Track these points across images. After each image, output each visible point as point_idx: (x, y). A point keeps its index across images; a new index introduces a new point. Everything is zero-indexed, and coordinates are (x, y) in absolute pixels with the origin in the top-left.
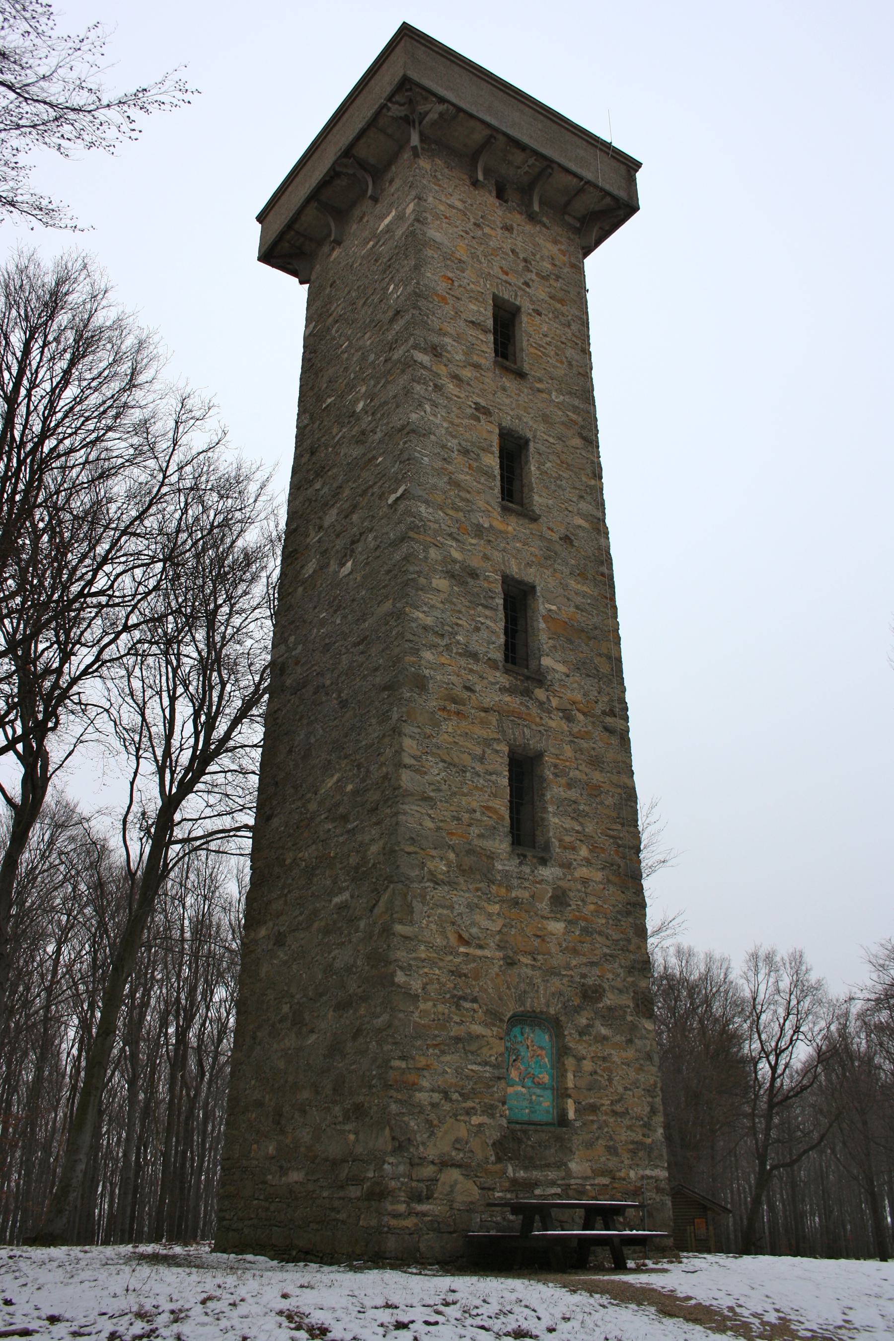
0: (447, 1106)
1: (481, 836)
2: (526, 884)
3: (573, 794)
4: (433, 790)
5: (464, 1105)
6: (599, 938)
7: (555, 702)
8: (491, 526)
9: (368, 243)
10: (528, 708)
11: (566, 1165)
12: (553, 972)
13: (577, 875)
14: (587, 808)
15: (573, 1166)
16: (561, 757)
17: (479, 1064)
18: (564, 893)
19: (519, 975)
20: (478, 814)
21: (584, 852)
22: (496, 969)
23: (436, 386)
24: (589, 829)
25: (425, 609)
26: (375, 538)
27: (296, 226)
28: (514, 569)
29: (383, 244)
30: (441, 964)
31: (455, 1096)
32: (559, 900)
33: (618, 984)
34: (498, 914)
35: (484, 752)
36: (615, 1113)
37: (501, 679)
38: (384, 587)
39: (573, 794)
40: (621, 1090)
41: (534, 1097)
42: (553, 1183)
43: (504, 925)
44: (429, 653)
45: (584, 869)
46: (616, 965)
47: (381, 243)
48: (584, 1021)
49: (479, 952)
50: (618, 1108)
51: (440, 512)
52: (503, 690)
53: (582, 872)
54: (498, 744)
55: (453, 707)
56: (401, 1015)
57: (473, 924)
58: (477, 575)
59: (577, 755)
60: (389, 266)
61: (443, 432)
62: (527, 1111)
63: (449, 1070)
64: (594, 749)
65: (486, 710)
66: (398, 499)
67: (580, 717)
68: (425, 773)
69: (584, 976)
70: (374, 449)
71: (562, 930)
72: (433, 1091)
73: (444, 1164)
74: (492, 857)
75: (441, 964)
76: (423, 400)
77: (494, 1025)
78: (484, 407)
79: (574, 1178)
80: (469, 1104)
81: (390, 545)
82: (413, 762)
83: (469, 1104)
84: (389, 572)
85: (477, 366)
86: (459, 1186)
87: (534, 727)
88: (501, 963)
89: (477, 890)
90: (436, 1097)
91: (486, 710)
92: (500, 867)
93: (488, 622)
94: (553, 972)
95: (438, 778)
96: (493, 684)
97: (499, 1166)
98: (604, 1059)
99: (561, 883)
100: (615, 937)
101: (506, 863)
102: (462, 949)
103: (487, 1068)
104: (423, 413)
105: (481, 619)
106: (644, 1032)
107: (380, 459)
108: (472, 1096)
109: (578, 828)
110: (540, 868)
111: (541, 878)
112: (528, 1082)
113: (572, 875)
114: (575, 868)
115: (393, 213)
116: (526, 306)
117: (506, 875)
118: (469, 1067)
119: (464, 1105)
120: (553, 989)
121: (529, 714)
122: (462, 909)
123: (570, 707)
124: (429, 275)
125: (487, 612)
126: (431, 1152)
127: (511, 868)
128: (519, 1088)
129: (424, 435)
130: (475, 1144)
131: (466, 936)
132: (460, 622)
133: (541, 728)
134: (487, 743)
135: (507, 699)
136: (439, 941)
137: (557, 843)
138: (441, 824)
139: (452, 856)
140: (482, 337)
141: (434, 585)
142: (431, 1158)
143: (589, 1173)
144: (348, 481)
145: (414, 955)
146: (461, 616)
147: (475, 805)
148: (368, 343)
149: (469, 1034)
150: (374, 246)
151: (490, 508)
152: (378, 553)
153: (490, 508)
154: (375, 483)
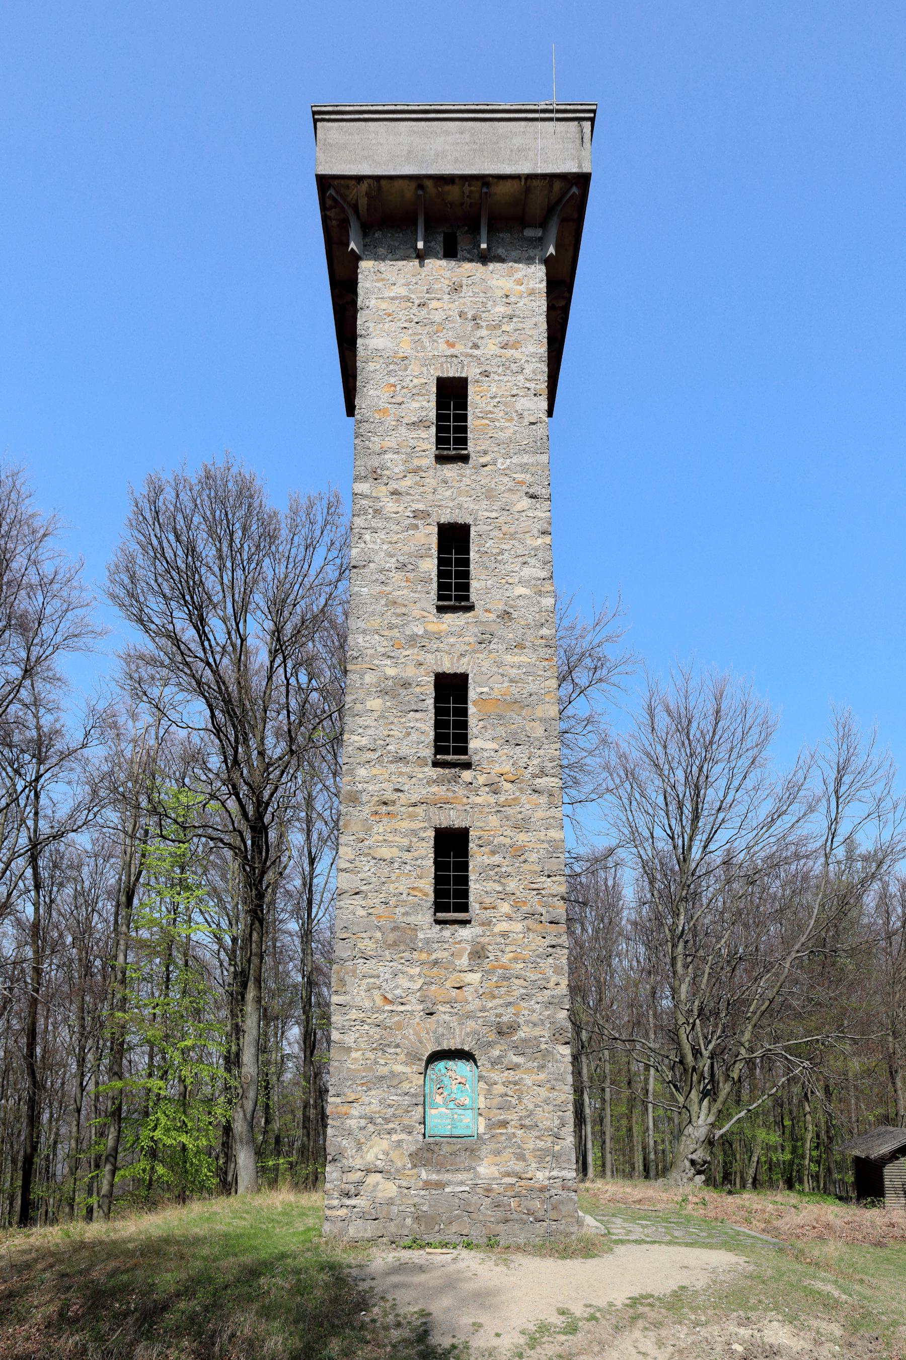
0: (371, 1128)
1: (406, 914)
2: (446, 946)
3: (496, 859)
5: (386, 1127)
6: (517, 981)
7: (482, 779)
8: (426, 631)
10: (454, 792)
11: (474, 1168)
12: (469, 1016)
13: (497, 929)
14: (509, 869)
15: (481, 1170)
16: (487, 828)
17: (400, 1095)
18: (483, 948)
19: (438, 1021)
20: (404, 895)
21: (505, 908)
22: (417, 1020)
23: (376, 511)
24: (512, 885)
25: (360, 731)
28: (448, 667)
30: (369, 1021)
31: (379, 1120)
32: (478, 954)
33: (535, 1017)
34: (419, 975)
35: (411, 841)
36: (522, 1126)
37: (430, 773)
39: (496, 859)
40: (531, 1106)
42: (462, 1183)
43: (425, 983)
44: (363, 769)
45: (504, 923)
46: (532, 1002)
48: (496, 1053)
49: (402, 1008)
50: (527, 1122)
51: (376, 637)
52: (431, 782)
53: (503, 926)
54: (425, 832)
55: (384, 809)
56: (336, 1064)
57: (396, 987)
58: (409, 684)
61: (382, 554)
68: (359, 872)
69: (499, 1015)
71: (479, 980)
72: (360, 1118)
73: (368, 1171)
74: (415, 928)
75: (369, 1021)
76: (363, 531)
77: (414, 1064)
78: (423, 512)
79: (482, 1179)
80: (391, 1125)
82: (348, 865)
83: (391, 1125)
86: (380, 1187)
87: (459, 807)
88: (422, 1013)
89: (402, 958)
90: (363, 1122)
93: (418, 725)
94: (469, 1016)
95: (369, 874)
97: (415, 1171)
98: (516, 1083)
99: (482, 940)
100: (533, 978)
101: (428, 931)
102: (388, 1008)
103: (406, 1097)
104: (363, 545)
105: (412, 725)
108: (393, 1119)
109: (500, 889)
110: (460, 930)
114: (495, 925)
117: (427, 941)
119: (386, 1127)
120: (468, 1030)
121: (457, 798)
122: (387, 976)
123: (498, 779)
125: (418, 715)
126: (358, 1163)
127: (433, 936)
129: (364, 566)
130: (394, 1155)
131: (389, 996)
132: (391, 733)
133: (467, 807)
134: (414, 832)
135: (434, 789)
136: (367, 1004)
137: (477, 906)
138: (370, 911)
139: (378, 935)
141: (368, 708)
142: (358, 1167)
145: (348, 1017)
146: (393, 727)
147: (401, 889)
149: (391, 1072)
151: (426, 614)
153: (426, 614)
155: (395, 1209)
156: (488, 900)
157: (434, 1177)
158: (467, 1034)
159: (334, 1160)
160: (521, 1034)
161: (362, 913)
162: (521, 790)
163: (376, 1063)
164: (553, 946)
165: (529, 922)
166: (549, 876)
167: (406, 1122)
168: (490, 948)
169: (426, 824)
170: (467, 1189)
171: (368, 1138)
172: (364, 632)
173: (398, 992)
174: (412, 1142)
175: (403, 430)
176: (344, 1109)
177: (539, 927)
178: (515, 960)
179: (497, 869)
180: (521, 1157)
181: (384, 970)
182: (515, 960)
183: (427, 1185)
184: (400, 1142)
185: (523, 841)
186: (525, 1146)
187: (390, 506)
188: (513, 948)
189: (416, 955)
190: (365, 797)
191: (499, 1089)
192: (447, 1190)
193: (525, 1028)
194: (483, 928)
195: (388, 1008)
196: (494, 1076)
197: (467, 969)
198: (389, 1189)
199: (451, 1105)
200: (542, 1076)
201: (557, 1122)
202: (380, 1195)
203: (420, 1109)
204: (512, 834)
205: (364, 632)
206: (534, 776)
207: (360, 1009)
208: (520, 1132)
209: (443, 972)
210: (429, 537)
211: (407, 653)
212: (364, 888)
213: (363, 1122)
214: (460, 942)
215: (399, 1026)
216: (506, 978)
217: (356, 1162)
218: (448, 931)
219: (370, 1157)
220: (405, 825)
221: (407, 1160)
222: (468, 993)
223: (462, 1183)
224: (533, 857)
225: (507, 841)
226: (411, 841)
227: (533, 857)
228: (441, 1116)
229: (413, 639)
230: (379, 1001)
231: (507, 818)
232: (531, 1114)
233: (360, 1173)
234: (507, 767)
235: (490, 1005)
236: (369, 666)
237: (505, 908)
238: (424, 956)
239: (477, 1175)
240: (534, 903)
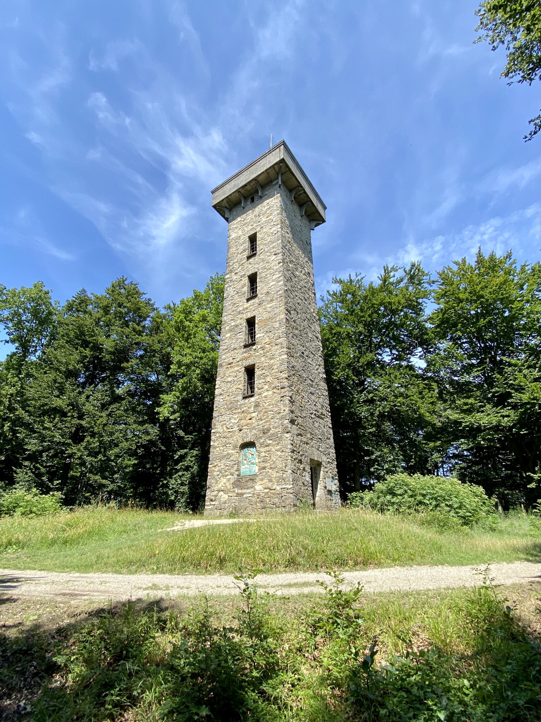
3: (264, 371)
6: (270, 413)
7: (259, 347)
12: (254, 428)
13: (263, 395)
14: (267, 374)
18: (259, 403)
24: (268, 379)
32: (257, 405)
33: (276, 425)
36: (271, 468)
42: (249, 493)
48: (263, 440)
49: (232, 430)
50: (273, 466)
55: (229, 366)
65: (238, 362)
69: (263, 426)
73: (219, 491)
83: (227, 473)
90: (218, 473)
94: (254, 428)
98: (269, 451)
106: (285, 438)
112: (249, 463)
117: (241, 405)
126: (216, 488)
130: (227, 484)
134: (238, 371)
135: (245, 355)
136: (221, 431)
143: (262, 489)
155: (227, 505)
156: (260, 386)
157: (240, 491)
158: (253, 435)
159: (209, 488)
160: (271, 432)
161: (222, 400)
162: (272, 346)
163: (223, 451)
164: (283, 397)
165: (275, 390)
166: (281, 372)
167: (232, 471)
171: (220, 478)
172: (226, 316)
173: (231, 424)
174: (233, 478)
175: (239, 255)
176: (213, 469)
177: (277, 391)
178: (269, 405)
180: (270, 481)
181: (227, 418)
182: (269, 405)
183: (238, 495)
184: (230, 478)
186: (272, 476)
187: (235, 277)
188: (269, 401)
189: (237, 411)
191: (263, 454)
193: (273, 430)
196: (262, 450)
198: (224, 497)
199: (249, 463)
200: (278, 447)
201: (284, 465)
202: (222, 499)
203: (236, 466)
205: (226, 316)
206: (276, 340)
207: (219, 433)
208: (270, 471)
209: (245, 414)
210: (246, 281)
213: (218, 473)
215: (231, 437)
216: (266, 412)
217: (216, 487)
218: (247, 400)
219: (220, 486)
220: (236, 368)
221: (231, 486)
222: (253, 420)
223: (249, 493)
224: (275, 367)
227: (275, 367)
228: (246, 468)
229: (239, 313)
230: (225, 429)
231: (267, 357)
232: (274, 462)
233: (217, 492)
234: (267, 340)
235: (261, 423)
237: (266, 387)
238: (239, 410)
239: (255, 490)
240: (276, 383)
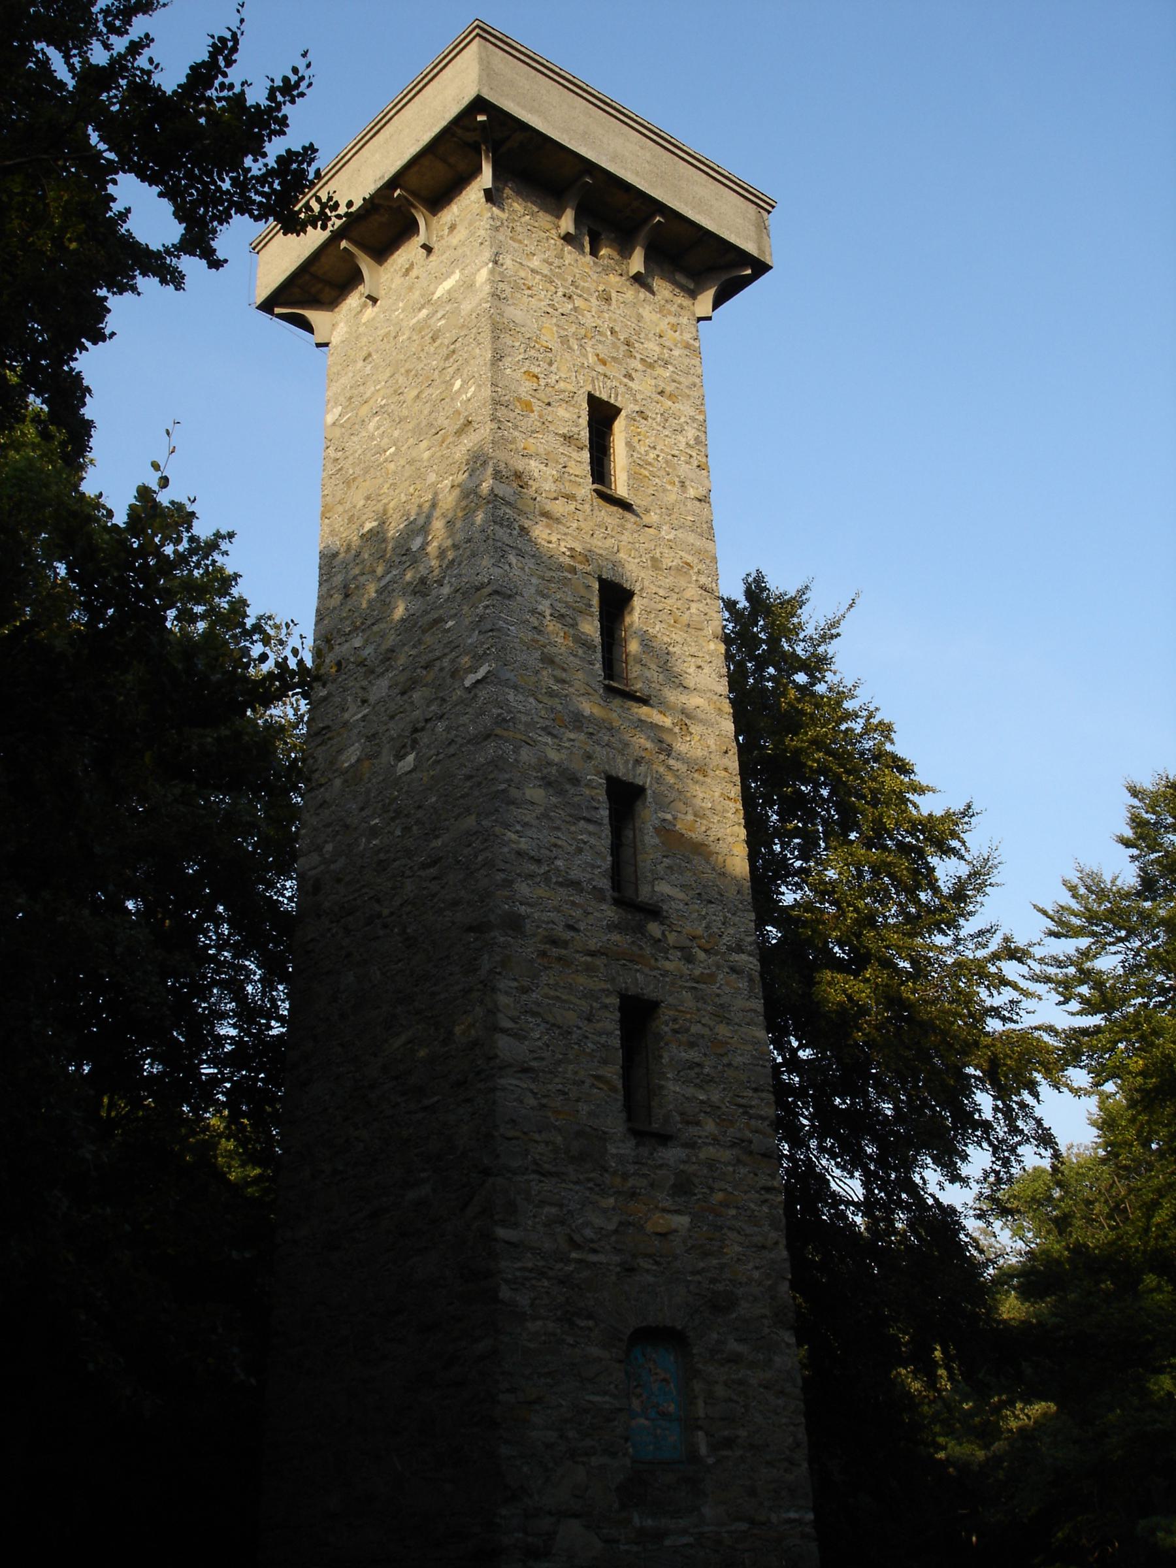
4: (535, 1059)
6: (729, 1234)
9: (420, 310)
10: (641, 948)
24: (715, 1097)
25: (518, 828)
26: (448, 729)
27: (313, 269)
29: (443, 316)
30: (551, 1273)
37: (609, 913)
38: (462, 797)
39: (693, 1055)
41: (659, 1431)
44: (524, 884)
45: (711, 1148)
47: (439, 315)
51: (531, 700)
52: (612, 927)
54: (607, 996)
55: (555, 952)
59: (700, 1005)
60: (454, 352)
61: (533, 590)
62: (651, 1447)
63: (564, 1403)
64: (718, 995)
65: (592, 954)
66: (478, 681)
67: (702, 955)
68: (525, 1038)
70: (441, 606)
71: (687, 1225)
75: (551, 1273)
76: (507, 548)
81: (469, 742)
84: (469, 778)
85: (569, 497)
87: (646, 970)
89: (589, 1180)
91: (592, 954)
92: (614, 1151)
93: (592, 841)
95: (539, 1043)
96: (600, 920)
102: (574, 1255)
103: (607, 1398)
104: (507, 567)
107: (450, 623)
110: (660, 1149)
111: (660, 1162)
113: (697, 1157)
114: (700, 1148)
115: (457, 276)
116: (628, 408)
118: (587, 1398)
124: (508, 371)
125: (591, 828)
128: (642, 1421)
131: (577, 1237)
132: (560, 843)
135: (616, 937)
137: (678, 1118)
138: (544, 1101)
140: (574, 455)
144: (404, 645)
145: (519, 1265)
146: (559, 834)
148: (426, 455)
150: (429, 317)
151: (591, 691)
152: (452, 750)
153: (591, 691)
154: (445, 655)
161: (532, 1102)
168: (696, 1181)
169: (608, 986)
170: (691, 1540)
179: (697, 1070)
185: (724, 1036)
190: (529, 927)
192: (667, 1542)
194: (687, 1151)
195: (574, 1255)
197: (673, 1208)
204: (712, 1023)
211: (572, 736)
212: (534, 1064)
214: (661, 1166)
220: (582, 980)
225: (706, 1031)
226: (591, 1006)
236: (524, 738)
